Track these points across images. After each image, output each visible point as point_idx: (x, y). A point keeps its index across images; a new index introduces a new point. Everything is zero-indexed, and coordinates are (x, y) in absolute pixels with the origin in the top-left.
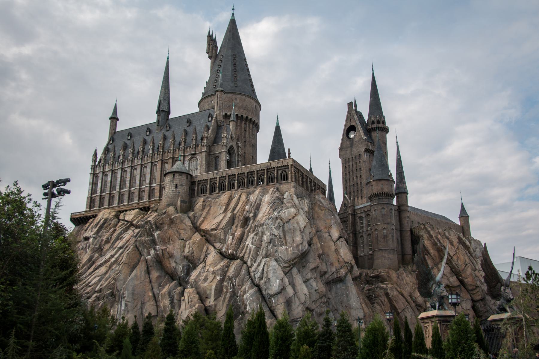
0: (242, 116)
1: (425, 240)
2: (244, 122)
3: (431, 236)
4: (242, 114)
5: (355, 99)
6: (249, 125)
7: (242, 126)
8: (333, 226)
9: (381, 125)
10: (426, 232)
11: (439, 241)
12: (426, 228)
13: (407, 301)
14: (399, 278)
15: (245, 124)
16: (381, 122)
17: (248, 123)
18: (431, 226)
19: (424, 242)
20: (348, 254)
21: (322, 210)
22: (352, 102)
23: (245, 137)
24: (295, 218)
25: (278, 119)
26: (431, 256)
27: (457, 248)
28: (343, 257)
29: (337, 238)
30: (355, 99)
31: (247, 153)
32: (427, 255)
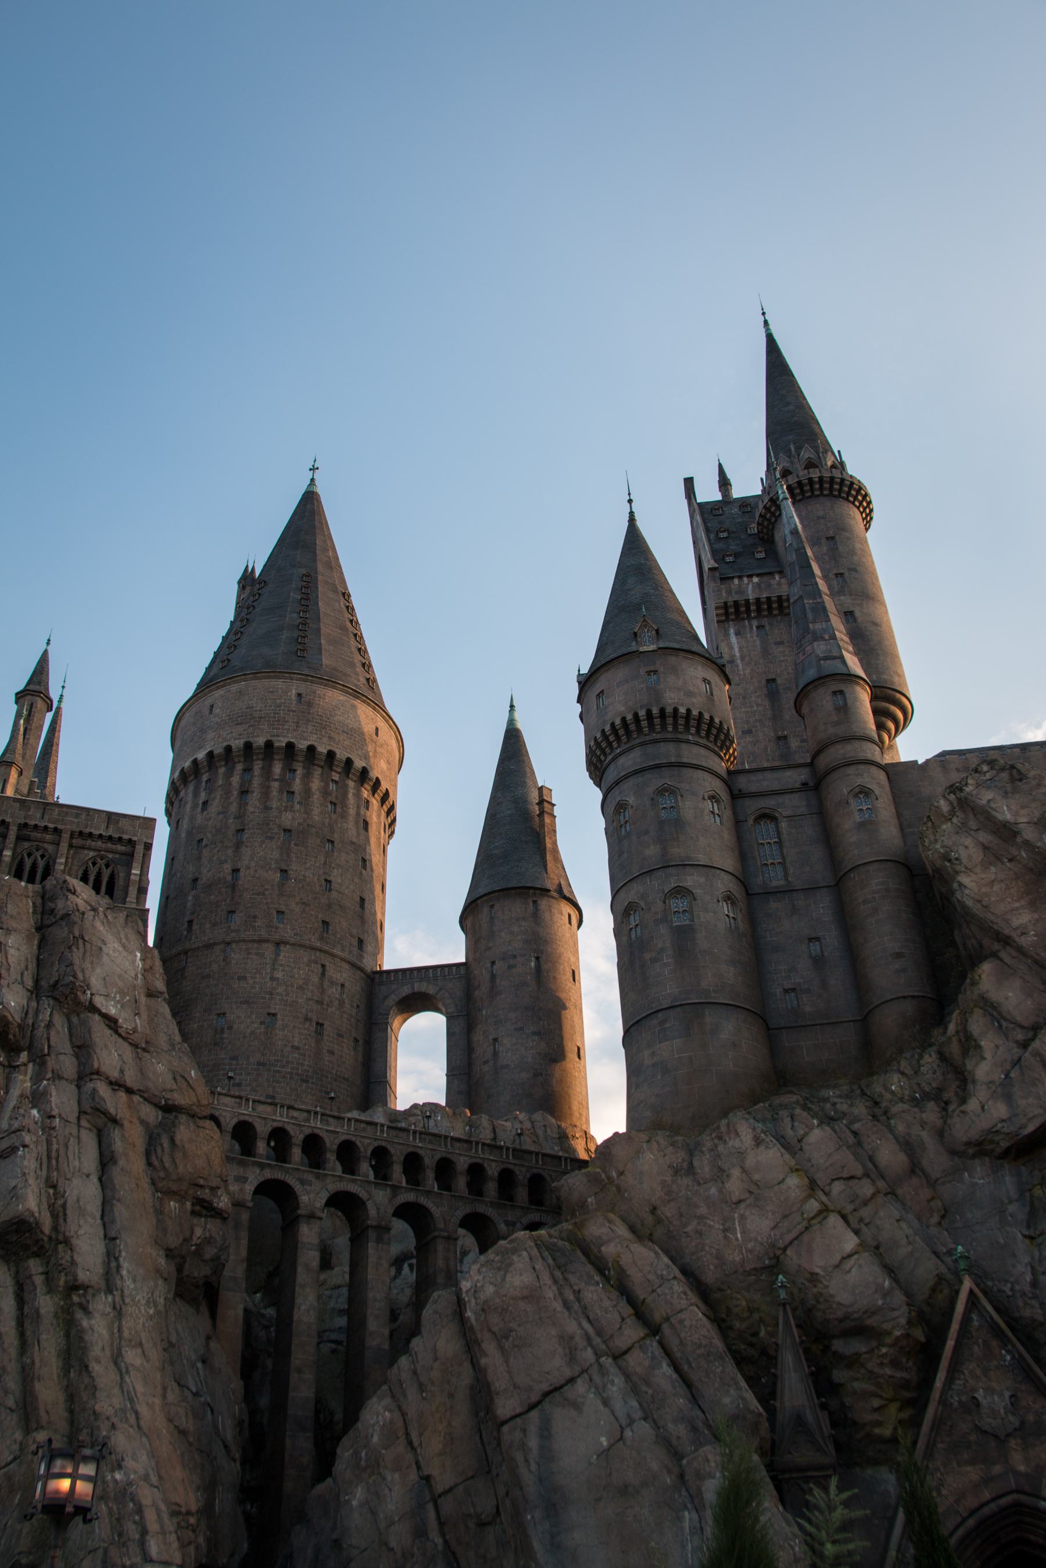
0: (228, 749)
1: (969, 870)
2: (239, 767)
3: (1007, 832)
6: (263, 768)
7: (230, 784)
10: (973, 824)
12: (965, 804)
13: (640, 1312)
14: (691, 1170)
15: (248, 770)
18: (1005, 775)
19: (960, 884)
22: (689, 483)
23: (239, 817)
25: (512, 706)
26: (1020, 950)
30: (720, 466)
31: (248, 868)
32: (994, 955)
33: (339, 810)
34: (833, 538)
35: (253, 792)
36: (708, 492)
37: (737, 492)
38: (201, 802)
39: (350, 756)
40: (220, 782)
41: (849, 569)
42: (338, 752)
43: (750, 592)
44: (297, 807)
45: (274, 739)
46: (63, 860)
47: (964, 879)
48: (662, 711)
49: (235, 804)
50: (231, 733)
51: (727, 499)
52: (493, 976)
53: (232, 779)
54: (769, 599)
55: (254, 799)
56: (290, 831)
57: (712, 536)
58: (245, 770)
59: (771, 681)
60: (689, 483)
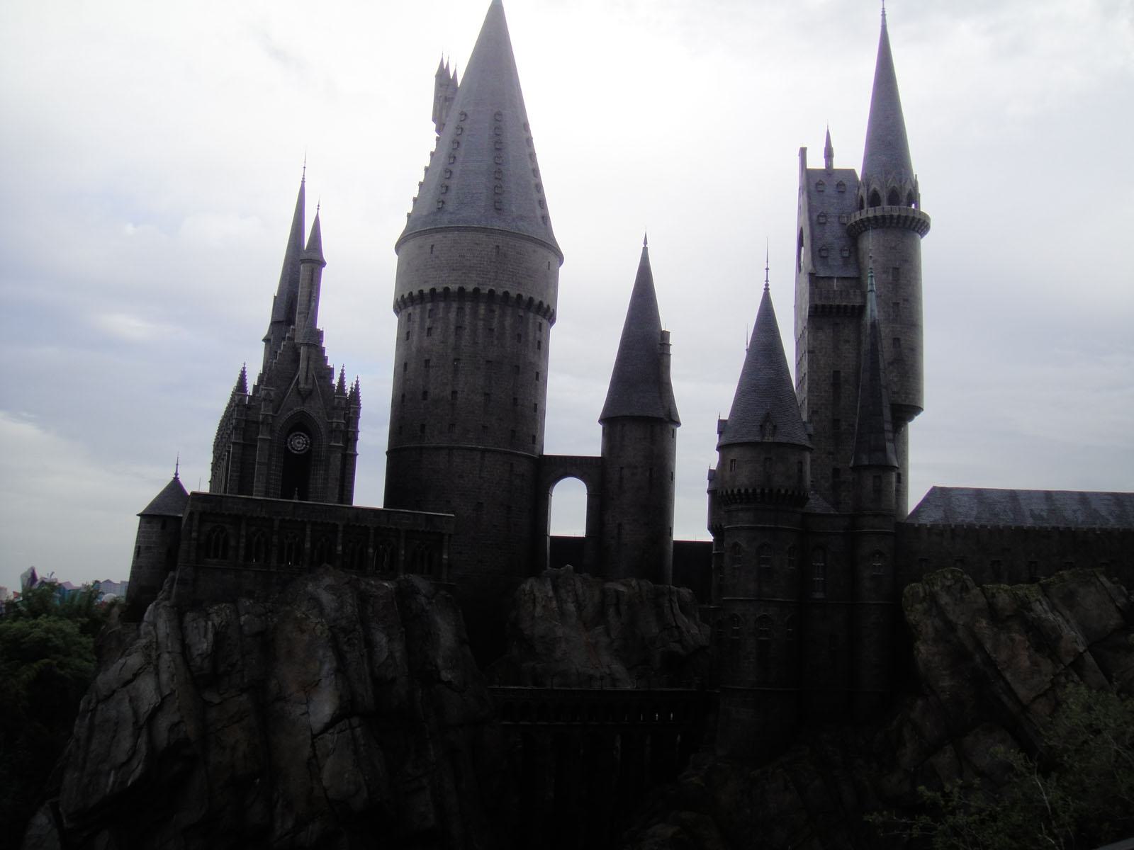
3: (951, 627)
4: (445, 286)
5: (828, 133)
8: (325, 682)
9: (885, 209)
11: (980, 645)
16: (883, 195)
17: (468, 306)
20: (346, 776)
21: (302, 631)
22: (803, 152)
24: (130, 687)
25: (645, 243)
27: (1072, 664)
28: (326, 783)
29: (327, 720)
30: (828, 133)
33: (523, 339)
34: (898, 269)
35: (465, 329)
36: (816, 162)
37: (837, 164)
38: (426, 327)
39: (532, 296)
40: (441, 315)
41: (905, 300)
42: (524, 294)
43: (835, 287)
44: (496, 342)
45: (480, 287)
46: (403, 552)
47: (922, 648)
48: (771, 490)
49: (452, 337)
50: (449, 276)
51: (829, 171)
52: (621, 478)
53: (450, 315)
54: (846, 306)
55: (467, 333)
56: (490, 362)
57: (815, 217)
58: (458, 308)
59: (836, 373)
60: (803, 152)
